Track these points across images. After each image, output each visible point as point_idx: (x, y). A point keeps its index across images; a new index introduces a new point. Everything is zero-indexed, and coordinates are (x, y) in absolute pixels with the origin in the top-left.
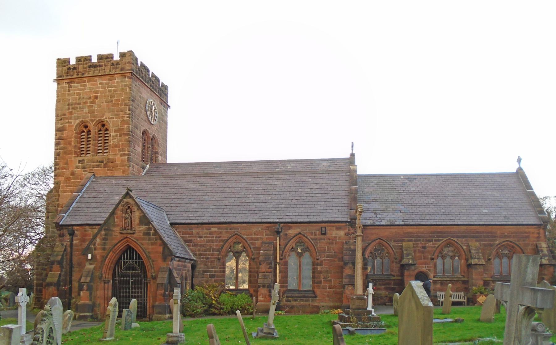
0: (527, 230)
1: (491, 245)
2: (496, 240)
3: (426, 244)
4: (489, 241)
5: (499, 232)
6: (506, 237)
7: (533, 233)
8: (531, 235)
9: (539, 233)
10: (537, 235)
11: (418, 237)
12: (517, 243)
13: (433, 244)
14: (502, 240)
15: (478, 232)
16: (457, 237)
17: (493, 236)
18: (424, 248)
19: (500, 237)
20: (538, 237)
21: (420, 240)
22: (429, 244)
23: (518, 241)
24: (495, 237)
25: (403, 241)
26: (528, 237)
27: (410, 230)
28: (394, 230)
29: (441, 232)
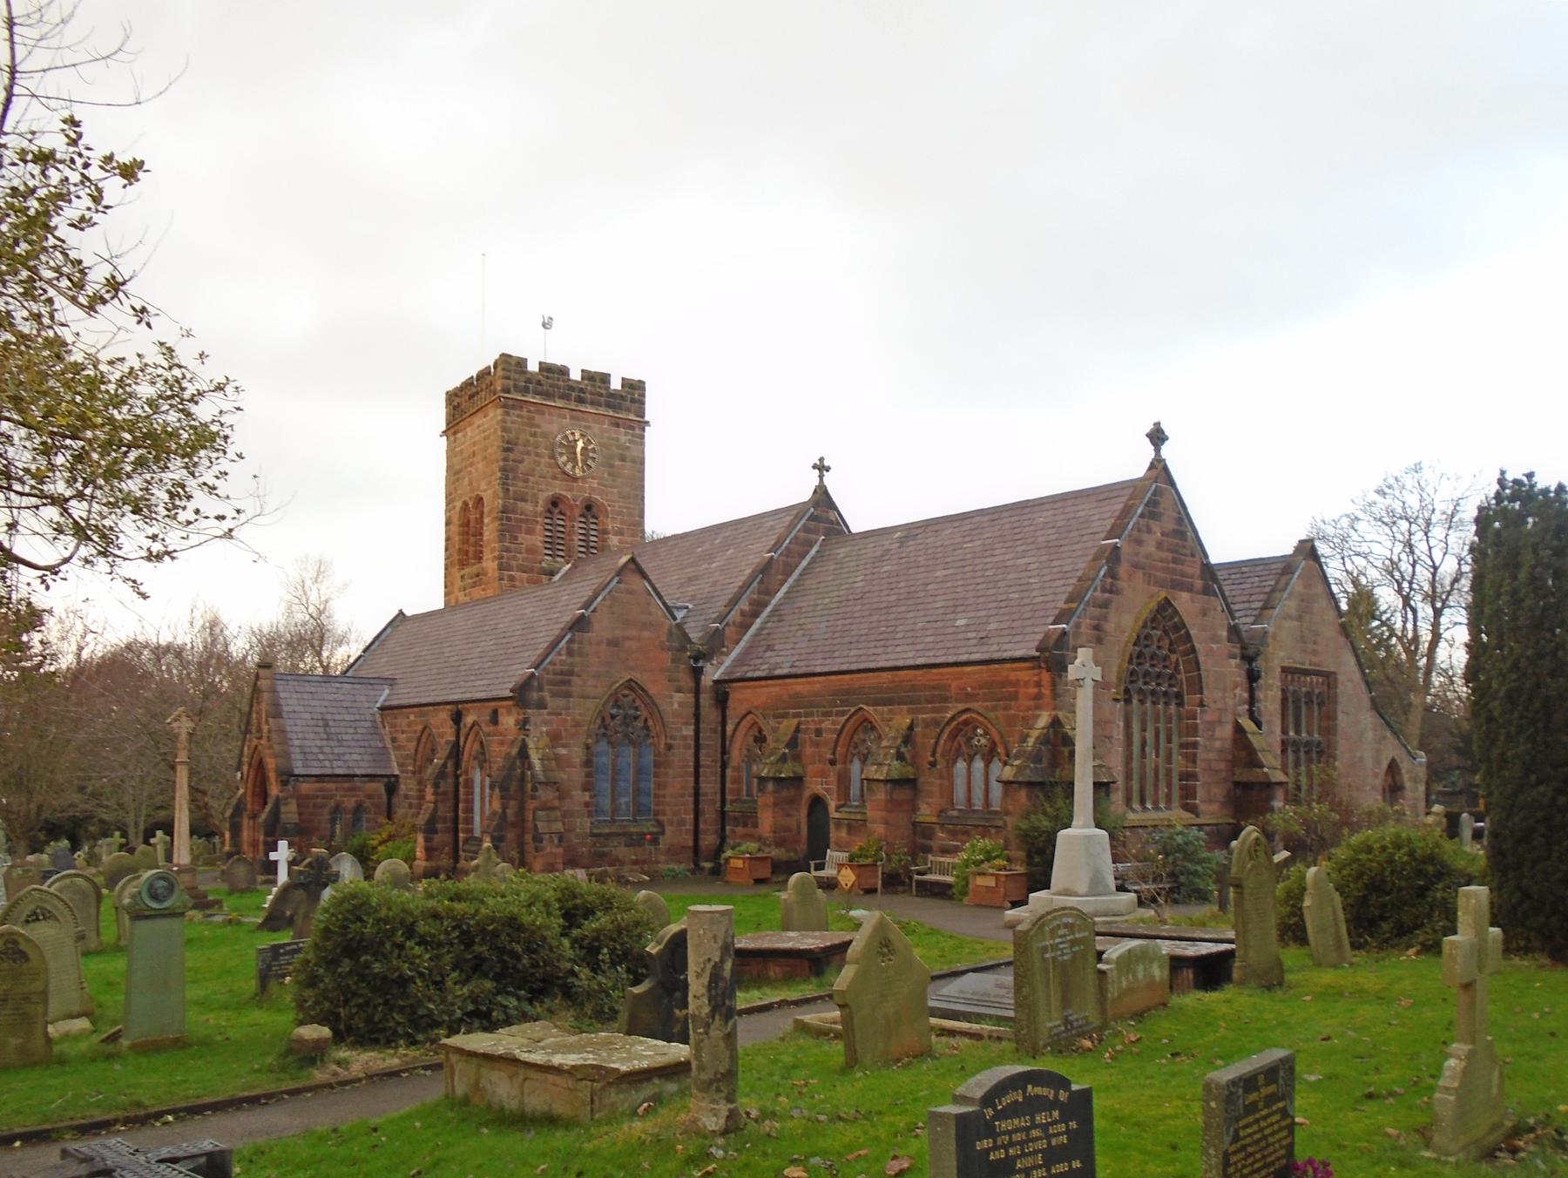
0: (1013, 676)
1: (935, 723)
2: (945, 710)
3: (821, 722)
4: (934, 710)
5: (954, 685)
6: (970, 697)
7: (1026, 684)
8: (1022, 691)
9: (1038, 685)
10: (1036, 690)
11: (811, 705)
12: (992, 715)
13: (834, 723)
14: (961, 706)
15: (913, 688)
16: (876, 703)
17: (940, 697)
18: (819, 732)
19: (957, 701)
20: (1038, 697)
21: (811, 714)
22: (827, 724)
23: (994, 709)
24: (945, 699)
25: (785, 716)
26: (1015, 696)
27: (798, 688)
28: (774, 689)
29: (848, 692)
